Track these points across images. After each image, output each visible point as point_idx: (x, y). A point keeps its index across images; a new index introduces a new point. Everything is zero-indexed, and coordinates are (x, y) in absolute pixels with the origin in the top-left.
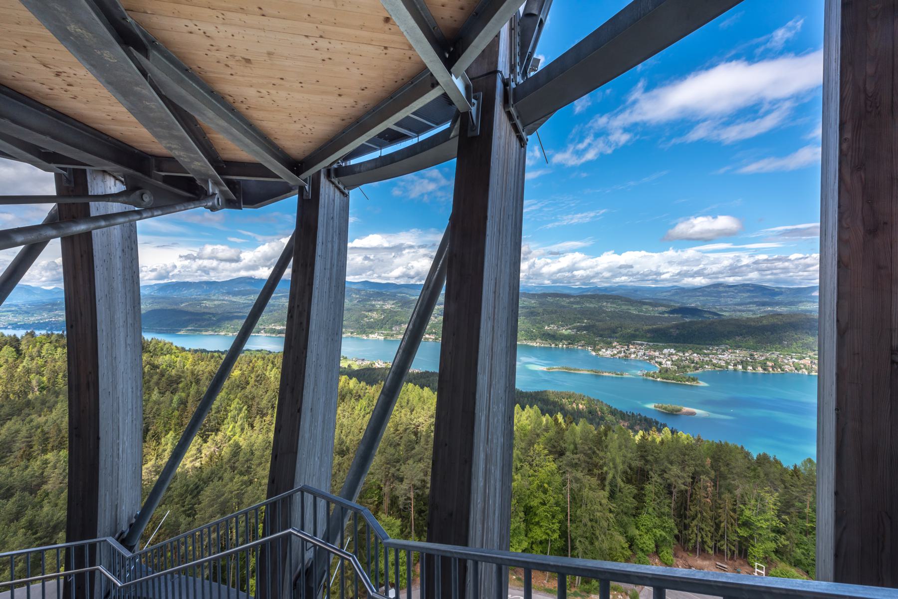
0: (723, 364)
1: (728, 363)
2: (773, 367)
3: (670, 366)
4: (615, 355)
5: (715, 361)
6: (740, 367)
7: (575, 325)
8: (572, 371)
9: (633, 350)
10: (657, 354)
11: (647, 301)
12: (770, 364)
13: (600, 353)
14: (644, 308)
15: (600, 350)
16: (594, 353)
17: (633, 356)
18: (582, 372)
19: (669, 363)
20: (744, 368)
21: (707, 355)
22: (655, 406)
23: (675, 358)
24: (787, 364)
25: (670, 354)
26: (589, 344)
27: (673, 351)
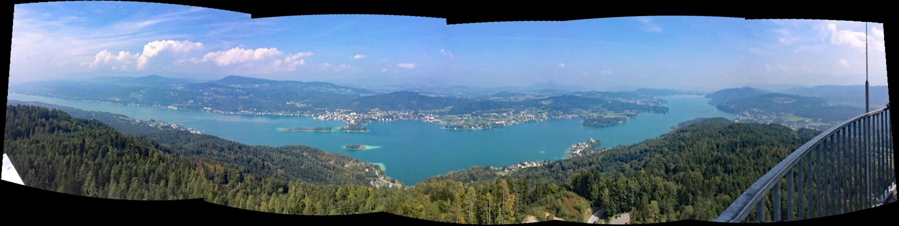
0: (376, 118)
1: (378, 118)
2: (395, 118)
3: (353, 123)
4: (326, 118)
5: (373, 118)
6: (383, 119)
7: (304, 101)
8: (303, 131)
9: (336, 115)
10: (347, 116)
11: (343, 85)
12: (394, 116)
13: (319, 118)
14: (341, 89)
15: (318, 116)
16: (315, 118)
17: (336, 118)
18: (308, 131)
19: (353, 121)
20: (385, 120)
21: (370, 114)
22: (347, 147)
23: (356, 117)
24: (400, 116)
25: (354, 116)
26: (312, 113)
27: (355, 114)
